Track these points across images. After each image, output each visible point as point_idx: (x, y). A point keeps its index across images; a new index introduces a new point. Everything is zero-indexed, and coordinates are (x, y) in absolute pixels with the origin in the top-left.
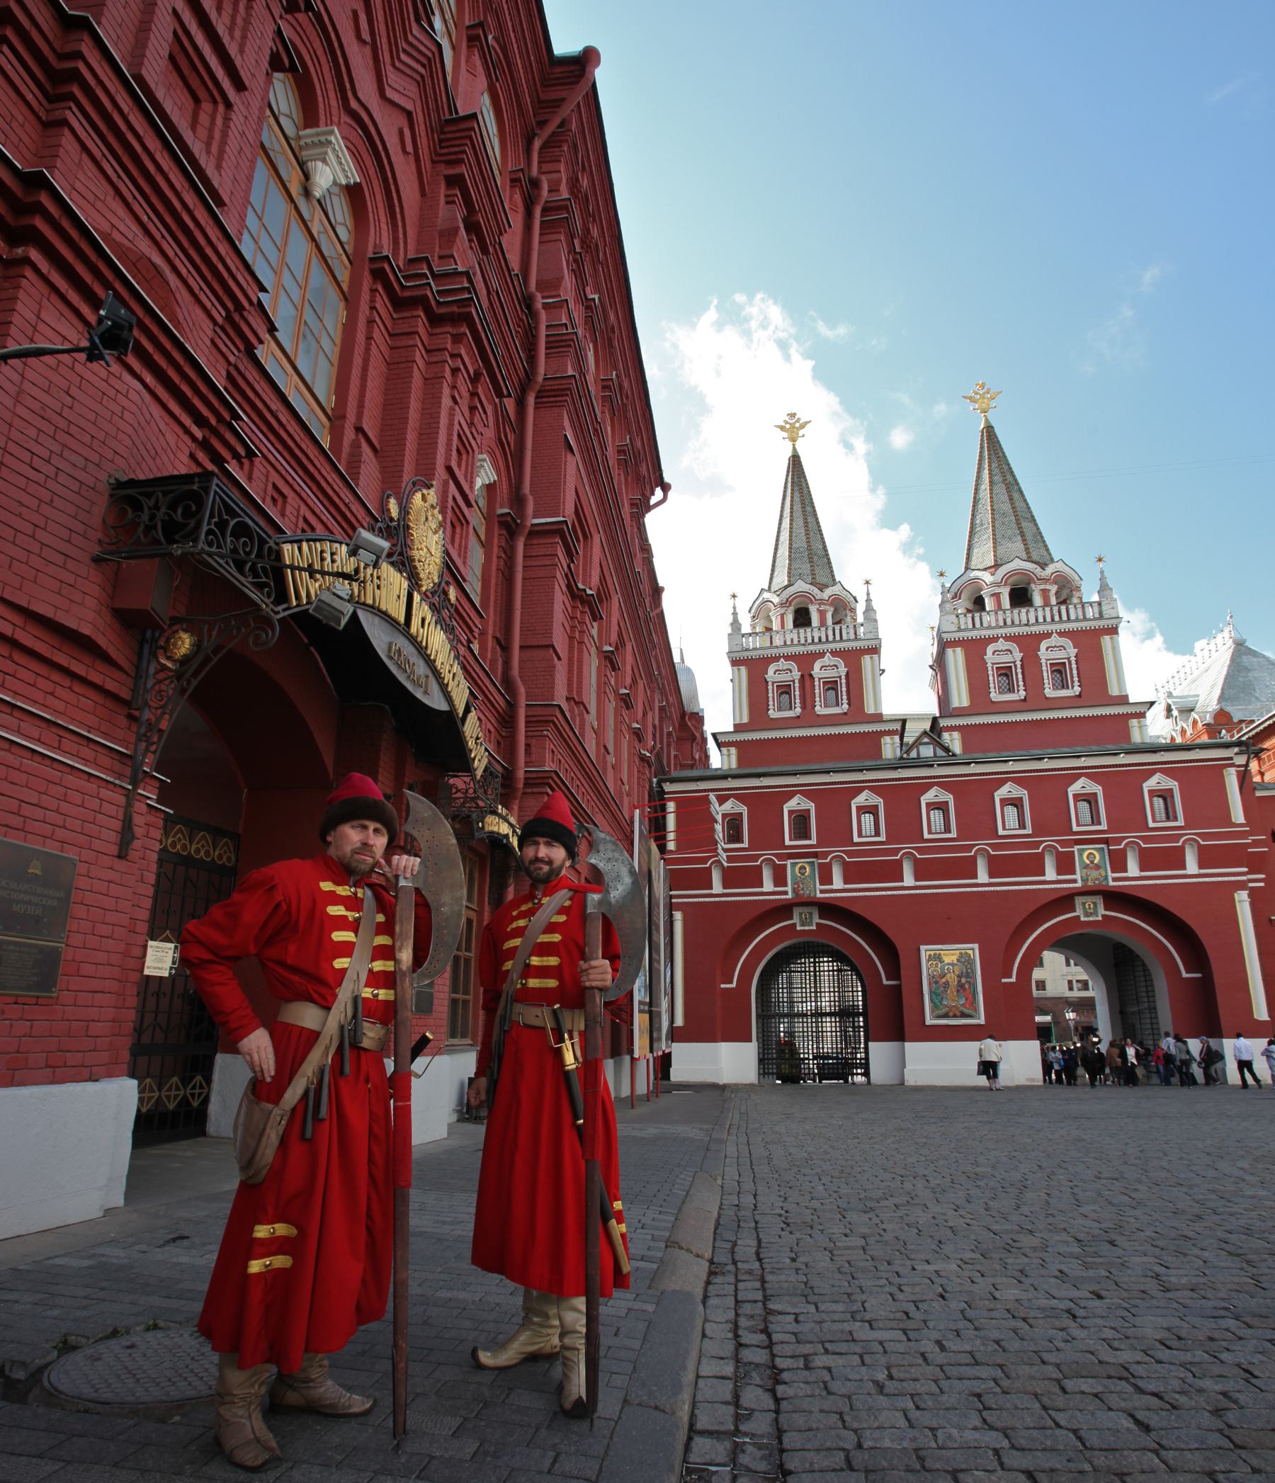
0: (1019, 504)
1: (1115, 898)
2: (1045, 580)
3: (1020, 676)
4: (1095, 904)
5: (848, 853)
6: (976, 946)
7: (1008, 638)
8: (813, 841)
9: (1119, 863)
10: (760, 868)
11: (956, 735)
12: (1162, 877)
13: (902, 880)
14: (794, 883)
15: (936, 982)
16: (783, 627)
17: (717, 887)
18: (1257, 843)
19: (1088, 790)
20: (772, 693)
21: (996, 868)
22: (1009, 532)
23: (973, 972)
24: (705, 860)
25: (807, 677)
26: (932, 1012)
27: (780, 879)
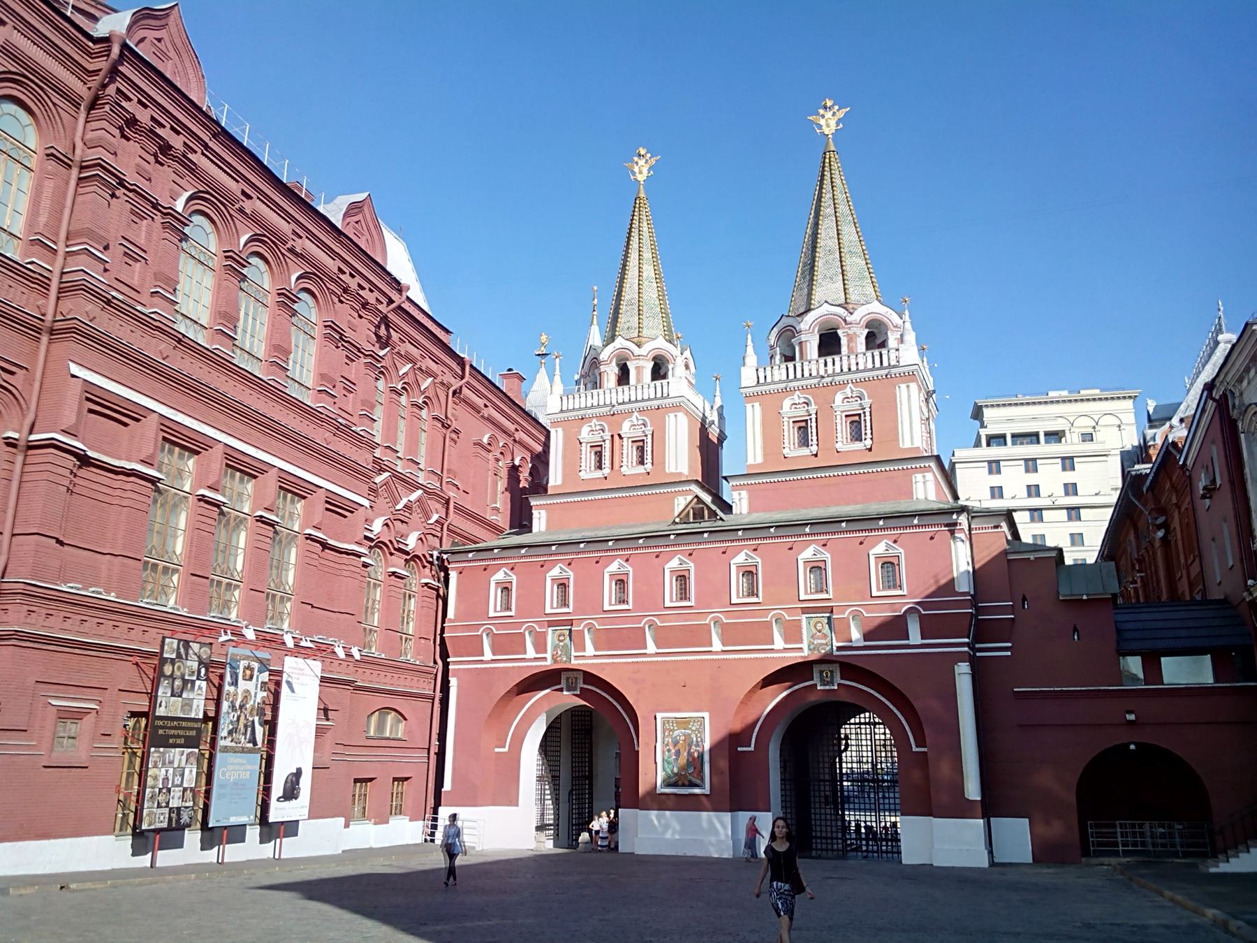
4: (832, 672)
11: (744, 494)
13: (646, 648)
14: (555, 648)
15: (669, 751)
19: (819, 557)
21: (730, 634)
22: (832, 272)
25: (616, 438)
27: (540, 646)
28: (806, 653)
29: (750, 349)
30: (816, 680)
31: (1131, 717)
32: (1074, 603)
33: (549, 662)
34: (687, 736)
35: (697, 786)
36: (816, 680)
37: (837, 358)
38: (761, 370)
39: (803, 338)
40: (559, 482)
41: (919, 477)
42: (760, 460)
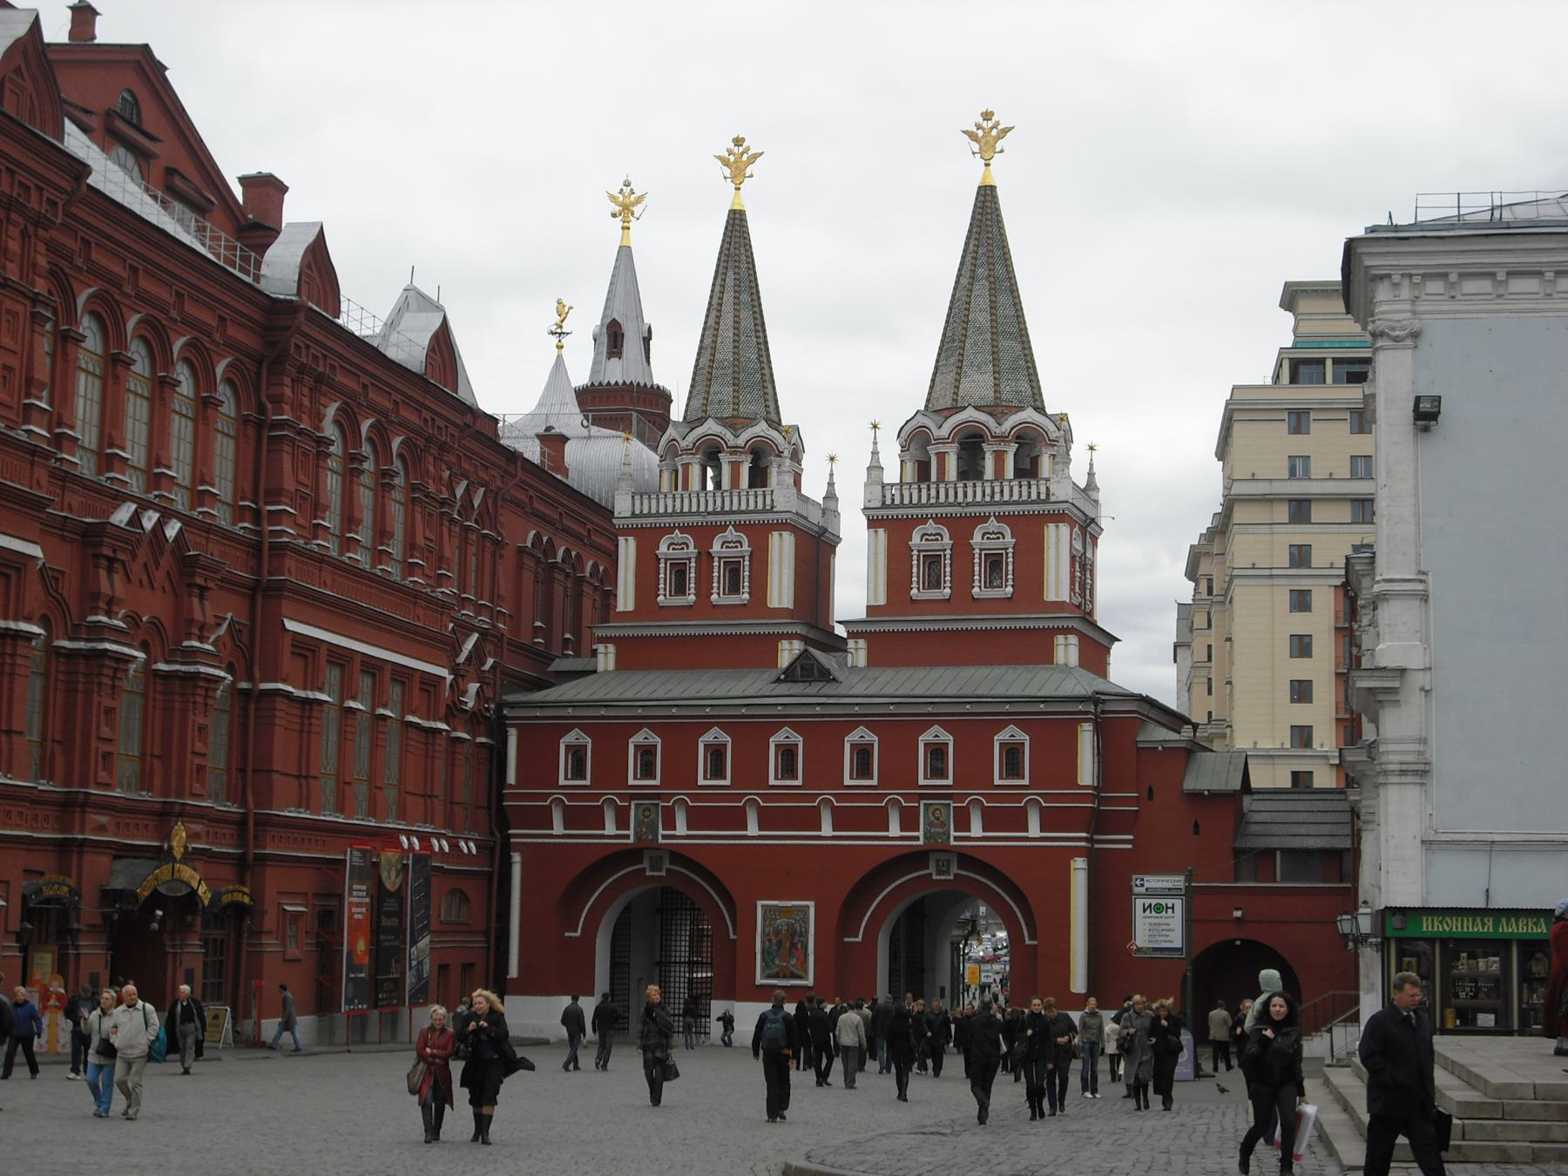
0: (1005, 311)
1: (967, 859)
2: (1002, 438)
5: (694, 797)
6: (811, 904)
7: (938, 520)
8: (657, 782)
9: (963, 823)
10: (601, 808)
11: (862, 643)
12: (1004, 838)
14: (638, 824)
16: (686, 487)
17: (558, 829)
18: (1125, 799)
20: (664, 574)
23: (807, 931)
24: (545, 797)
25: (704, 557)
26: (763, 971)
27: (622, 822)
28: (921, 842)
30: (932, 869)
31: (1238, 914)
32: (1196, 796)
33: (631, 840)
34: (790, 926)
35: (799, 977)
36: (932, 869)
37: (979, 484)
40: (631, 607)
41: (1060, 639)
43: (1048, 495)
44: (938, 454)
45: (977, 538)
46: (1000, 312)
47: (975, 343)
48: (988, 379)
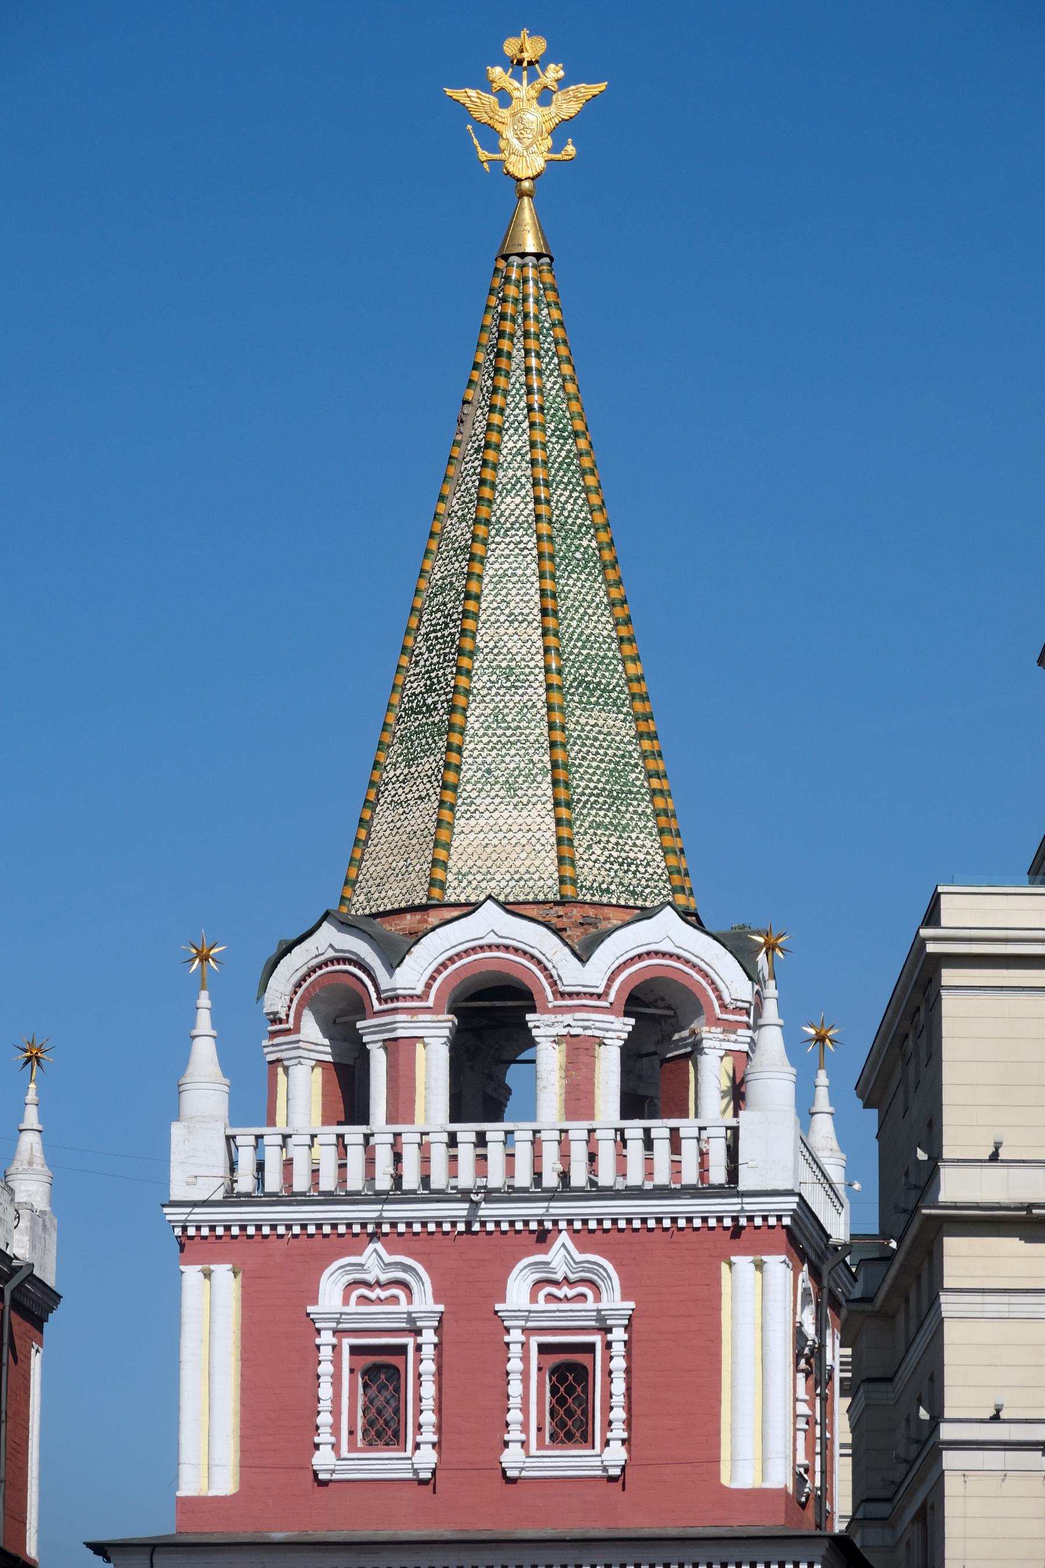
3: (429, 1390)
22: (514, 760)
29: (204, 1052)
38: (245, 1140)
39: (404, 1027)
42: (225, 1482)
43: (733, 1174)
44: (391, 1045)
45: (518, 1292)
46: (570, 625)
47: (496, 713)
48: (539, 820)
